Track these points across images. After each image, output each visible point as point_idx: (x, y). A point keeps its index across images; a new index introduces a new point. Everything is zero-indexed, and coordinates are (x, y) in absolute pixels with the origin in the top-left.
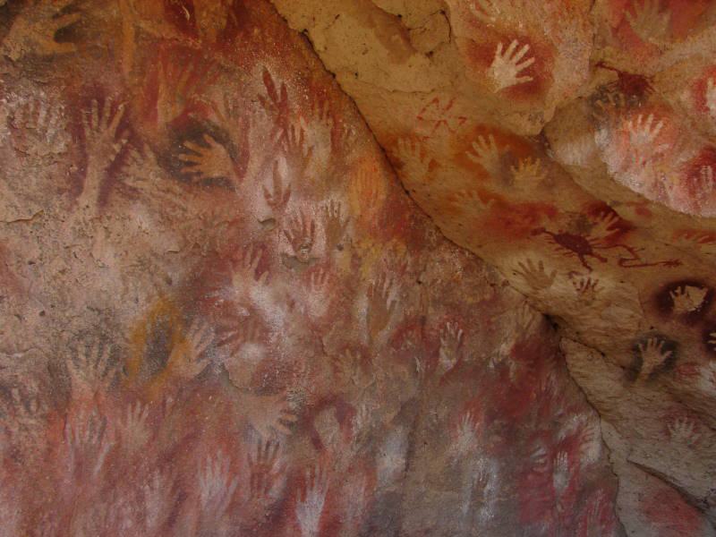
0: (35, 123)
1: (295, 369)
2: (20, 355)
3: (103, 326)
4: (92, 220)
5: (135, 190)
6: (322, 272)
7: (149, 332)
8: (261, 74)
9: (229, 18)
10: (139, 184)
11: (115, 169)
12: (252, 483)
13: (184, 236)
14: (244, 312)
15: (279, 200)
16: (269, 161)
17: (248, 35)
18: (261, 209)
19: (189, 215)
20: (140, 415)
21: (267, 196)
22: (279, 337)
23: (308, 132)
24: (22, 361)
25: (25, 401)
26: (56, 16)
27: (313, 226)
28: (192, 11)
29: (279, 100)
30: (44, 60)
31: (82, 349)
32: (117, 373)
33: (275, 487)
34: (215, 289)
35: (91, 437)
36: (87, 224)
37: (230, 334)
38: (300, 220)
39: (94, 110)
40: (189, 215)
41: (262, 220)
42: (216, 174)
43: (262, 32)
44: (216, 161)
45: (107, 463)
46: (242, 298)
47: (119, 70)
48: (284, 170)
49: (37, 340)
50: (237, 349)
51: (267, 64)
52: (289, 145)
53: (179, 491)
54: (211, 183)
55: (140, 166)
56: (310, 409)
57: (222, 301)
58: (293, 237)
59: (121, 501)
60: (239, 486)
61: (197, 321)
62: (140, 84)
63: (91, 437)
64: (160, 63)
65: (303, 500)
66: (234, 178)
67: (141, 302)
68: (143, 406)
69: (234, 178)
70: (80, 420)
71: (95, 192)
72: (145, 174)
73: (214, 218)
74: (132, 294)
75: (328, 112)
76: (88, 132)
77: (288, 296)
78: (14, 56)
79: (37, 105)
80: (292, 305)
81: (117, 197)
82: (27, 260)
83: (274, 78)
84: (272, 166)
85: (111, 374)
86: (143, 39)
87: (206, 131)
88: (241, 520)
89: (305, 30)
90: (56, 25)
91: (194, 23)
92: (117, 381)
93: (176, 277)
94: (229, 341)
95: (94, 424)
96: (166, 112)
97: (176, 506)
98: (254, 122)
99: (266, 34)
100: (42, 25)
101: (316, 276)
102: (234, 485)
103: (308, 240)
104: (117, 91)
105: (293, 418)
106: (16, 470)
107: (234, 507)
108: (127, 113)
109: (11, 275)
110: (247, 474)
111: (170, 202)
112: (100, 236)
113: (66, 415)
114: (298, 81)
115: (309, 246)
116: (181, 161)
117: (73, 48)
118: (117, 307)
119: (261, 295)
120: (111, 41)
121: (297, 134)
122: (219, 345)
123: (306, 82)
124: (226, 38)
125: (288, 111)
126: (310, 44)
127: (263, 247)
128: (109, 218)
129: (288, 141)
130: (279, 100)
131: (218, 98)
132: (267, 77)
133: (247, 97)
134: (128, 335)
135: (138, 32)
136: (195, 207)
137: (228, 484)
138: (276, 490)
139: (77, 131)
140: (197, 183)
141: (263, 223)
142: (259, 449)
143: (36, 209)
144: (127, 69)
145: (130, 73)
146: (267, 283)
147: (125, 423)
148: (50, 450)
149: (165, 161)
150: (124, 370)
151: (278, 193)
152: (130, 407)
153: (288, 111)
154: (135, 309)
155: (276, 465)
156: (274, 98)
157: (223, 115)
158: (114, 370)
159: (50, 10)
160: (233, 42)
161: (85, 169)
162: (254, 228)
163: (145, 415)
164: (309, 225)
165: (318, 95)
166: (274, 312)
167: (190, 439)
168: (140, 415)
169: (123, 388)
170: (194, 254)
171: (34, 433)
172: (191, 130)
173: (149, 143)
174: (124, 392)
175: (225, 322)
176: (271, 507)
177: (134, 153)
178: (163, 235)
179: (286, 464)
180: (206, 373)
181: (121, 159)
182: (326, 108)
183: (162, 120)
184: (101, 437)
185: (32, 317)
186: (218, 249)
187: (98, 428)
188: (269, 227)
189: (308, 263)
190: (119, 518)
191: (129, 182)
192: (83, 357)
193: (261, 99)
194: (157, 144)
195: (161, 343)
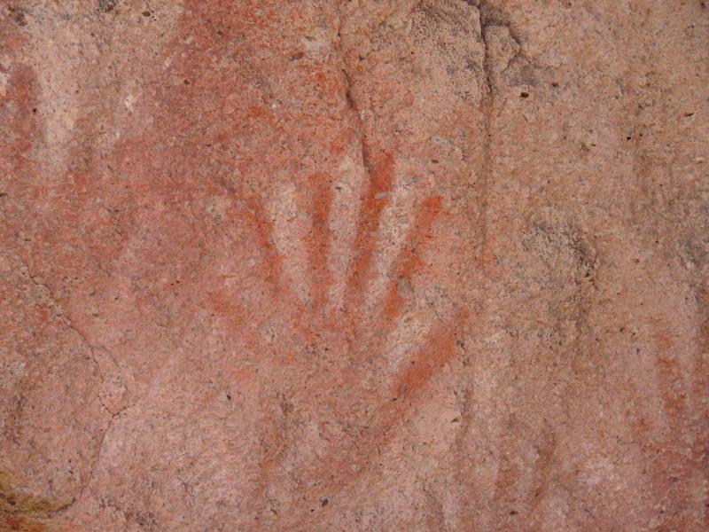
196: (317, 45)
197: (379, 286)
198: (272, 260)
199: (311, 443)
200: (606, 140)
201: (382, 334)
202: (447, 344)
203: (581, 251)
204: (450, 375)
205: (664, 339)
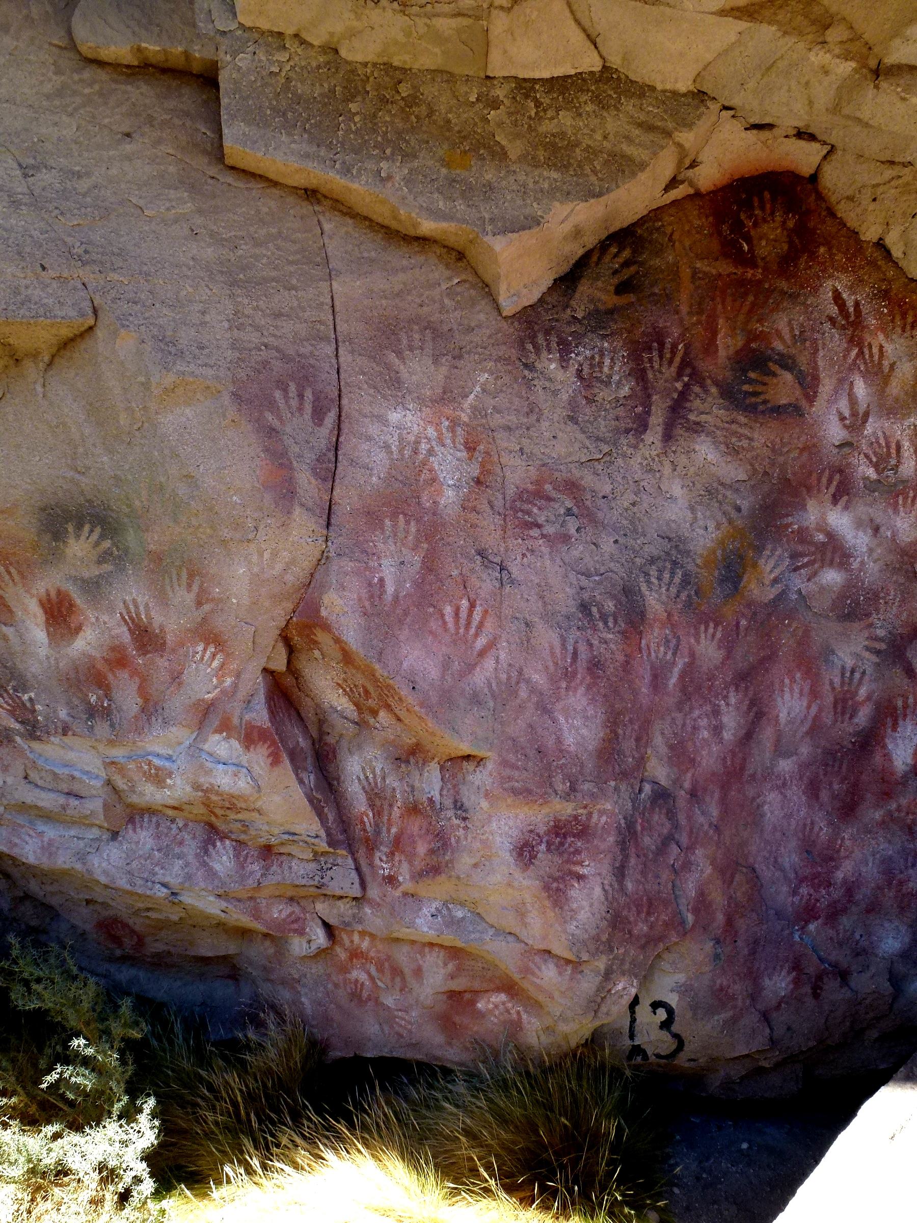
0: (601, 372)
1: (882, 595)
2: (597, 578)
3: (674, 552)
4: (658, 455)
5: (698, 423)
6: (911, 494)
7: (720, 558)
8: (830, 294)
9: (791, 243)
10: (703, 418)
11: (678, 408)
12: (835, 707)
13: (751, 465)
14: (821, 537)
15: (856, 421)
16: (843, 383)
17: (813, 256)
18: (835, 432)
19: (755, 444)
20: (713, 636)
21: (843, 419)
22: (862, 563)
23: (889, 348)
24: (599, 583)
25: (604, 617)
26: (615, 272)
27: (899, 447)
28: (749, 241)
29: (852, 318)
30: (606, 313)
31: (653, 572)
32: (689, 596)
33: (861, 714)
34: (787, 515)
35: (666, 653)
36: (653, 460)
37: (806, 560)
38: (882, 442)
39: (655, 353)
40: (755, 444)
41: (837, 444)
42: (783, 402)
43: (830, 249)
44: (783, 388)
45: (682, 677)
46: (817, 524)
47: (677, 312)
48: (861, 389)
49: (612, 564)
50: (815, 574)
51: (840, 282)
52: (865, 363)
53: (755, 709)
54: (778, 410)
55: (703, 401)
56: (902, 638)
57: (796, 527)
58: (874, 460)
59: (696, 713)
60: (820, 710)
61: (770, 547)
62: (699, 322)
63: (666, 653)
64: (718, 299)
65: (894, 729)
66: (804, 403)
67: (710, 530)
68: (715, 628)
69: (804, 403)
70: (653, 637)
71: (660, 429)
72: (709, 408)
73: (783, 444)
74: (701, 523)
75: (913, 323)
76: (650, 375)
77: (871, 520)
78: (579, 315)
79: (602, 355)
80: (876, 530)
81: (681, 432)
82: (601, 495)
83: (845, 296)
84: (846, 387)
85: (683, 596)
86: (700, 278)
87: (770, 359)
88: (823, 743)
89: (881, 239)
90: (615, 281)
91: (753, 254)
92: (689, 604)
93: (745, 505)
94: (804, 566)
95: (668, 641)
96: (727, 344)
97: (753, 722)
98: (824, 344)
99: (834, 251)
100: (603, 282)
101: (905, 499)
102: (814, 710)
103: (893, 462)
104: (676, 332)
105: (883, 646)
106: (599, 677)
107: (815, 729)
108: (687, 353)
109: (587, 508)
110: (829, 699)
111: (735, 433)
112: (667, 470)
113: (641, 633)
114: (875, 295)
115: (895, 468)
116: (746, 392)
117: (632, 298)
118: (687, 535)
119: (840, 520)
120: (668, 286)
121: (875, 350)
122: (795, 570)
123: (885, 294)
124: (786, 264)
125: (864, 327)
126: (888, 252)
127: (841, 471)
128: (674, 452)
129: (864, 358)
130: (852, 318)
131: (783, 324)
132: (837, 297)
133: (815, 320)
134: (699, 561)
135: (695, 272)
136: (761, 437)
137: (809, 707)
138: (863, 717)
139: (639, 375)
140: (763, 412)
141: (840, 446)
142: (843, 674)
143: (606, 448)
144: (684, 309)
145: (689, 313)
146: (846, 508)
147: (698, 642)
148: (627, 662)
149: (729, 394)
150: (696, 593)
151: (854, 414)
152: (702, 628)
153: (864, 327)
154: (705, 535)
155: (863, 692)
156: (846, 316)
157: (789, 342)
158: (686, 593)
159: (609, 268)
160: (795, 266)
161: (650, 410)
162: (831, 455)
163: (719, 635)
164: (893, 446)
165: (900, 306)
166: (855, 537)
167: (767, 660)
168: (713, 636)
169: (697, 610)
170: (764, 482)
171: (612, 646)
172: (755, 360)
173: (710, 377)
174: (697, 610)
175: (800, 548)
176: (857, 734)
177: (697, 389)
178: (730, 466)
179: (874, 692)
180: (781, 597)
181: (684, 395)
182: (910, 319)
183: (722, 353)
184: (674, 654)
185: (607, 545)
186: (789, 476)
187: (672, 645)
188: (846, 450)
189: (895, 485)
190: (695, 728)
191: (692, 417)
192: (655, 581)
193: (831, 319)
194: (720, 378)
195: (733, 568)
196: (455, 573)
197: (472, 631)
198: (445, 623)
199: (456, 666)
200: (534, 598)
201: (474, 642)
202: (492, 645)
203: (527, 625)
204: (493, 651)
205: (552, 648)
